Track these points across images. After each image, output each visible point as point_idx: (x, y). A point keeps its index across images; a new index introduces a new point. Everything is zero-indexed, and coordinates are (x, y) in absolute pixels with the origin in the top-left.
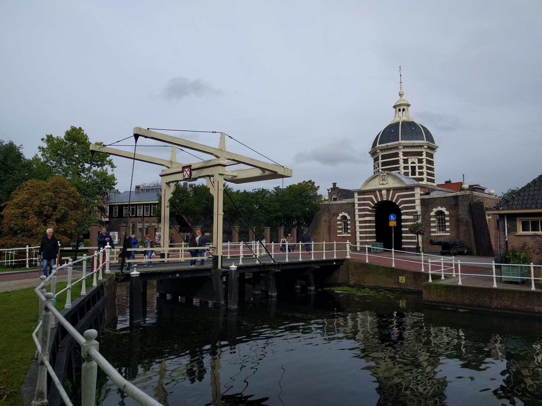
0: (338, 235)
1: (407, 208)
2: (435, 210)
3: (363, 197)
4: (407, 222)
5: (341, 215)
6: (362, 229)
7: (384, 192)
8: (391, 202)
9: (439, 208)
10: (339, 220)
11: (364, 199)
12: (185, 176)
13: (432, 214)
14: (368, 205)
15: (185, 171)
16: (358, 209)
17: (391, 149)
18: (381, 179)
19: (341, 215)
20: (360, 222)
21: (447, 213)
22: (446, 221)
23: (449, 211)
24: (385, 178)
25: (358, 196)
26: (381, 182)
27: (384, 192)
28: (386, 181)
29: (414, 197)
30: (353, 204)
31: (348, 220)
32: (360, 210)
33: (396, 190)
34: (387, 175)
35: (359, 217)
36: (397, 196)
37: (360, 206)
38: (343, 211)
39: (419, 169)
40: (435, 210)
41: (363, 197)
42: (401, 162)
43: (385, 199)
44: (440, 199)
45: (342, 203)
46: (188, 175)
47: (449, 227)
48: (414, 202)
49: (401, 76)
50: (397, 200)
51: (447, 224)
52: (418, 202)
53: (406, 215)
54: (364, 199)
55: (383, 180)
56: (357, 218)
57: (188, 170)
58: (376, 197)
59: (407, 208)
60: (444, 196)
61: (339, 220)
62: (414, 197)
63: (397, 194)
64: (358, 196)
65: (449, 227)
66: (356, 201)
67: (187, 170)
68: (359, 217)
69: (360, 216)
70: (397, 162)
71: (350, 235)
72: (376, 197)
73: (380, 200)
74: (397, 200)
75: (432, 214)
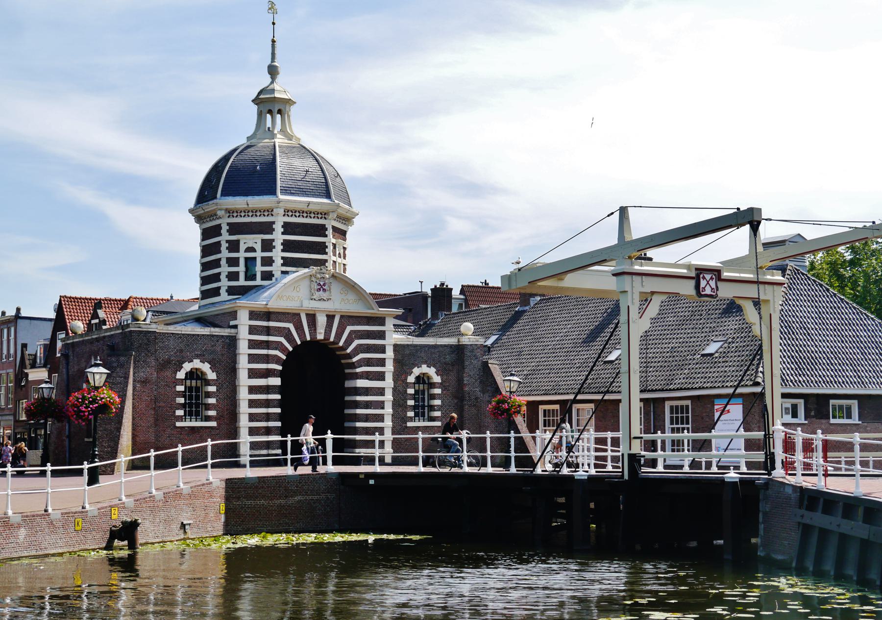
0: (178, 424)
1: (369, 362)
2: (416, 371)
3: (265, 324)
4: (367, 395)
5: (187, 367)
6: (256, 407)
7: (322, 320)
8: (314, 342)
9: (424, 369)
10: (180, 382)
11: (268, 331)
12: (704, 288)
13: (411, 379)
14: (278, 346)
15: (704, 278)
16: (249, 355)
17: (309, 213)
18: (317, 287)
19: (187, 367)
20: (252, 390)
21: (437, 379)
22: (414, 397)
23: (442, 376)
24: (324, 285)
25: (250, 319)
26: (317, 295)
27: (322, 320)
28: (327, 293)
29: (384, 339)
30: (233, 342)
31: (208, 383)
32: (252, 358)
33: (348, 319)
34: (332, 280)
35: (250, 377)
36: (350, 333)
37: (254, 348)
38: (197, 357)
39: (263, 265)
40: (416, 371)
41: (265, 324)
42: (278, 246)
43: (320, 336)
44: (427, 349)
45: (194, 335)
46: (712, 289)
47: (440, 408)
48: (382, 349)
49: (274, 24)
50: (349, 342)
51: (411, 403)
52: (390, 354)
53: (367, 379)
54: (268, 331)
55: (319, 290)
56: (244, 381)
57: (712, 278)
58: (299, 328)
59: (369, 362)
60: (433, 343)
61: (180, 382)
62: (384, 339)
63: (349, 329)
64: (250, 319)
65: (440, 408)
66: (244, 336)
67: (708, 277)
68: (250, 377)
69: (253, 374)
70: (288, 246)
71: (214, 424)
72: (299, 328)
73: (308, 338)
74: (349, 342)
75: (411, 379)
